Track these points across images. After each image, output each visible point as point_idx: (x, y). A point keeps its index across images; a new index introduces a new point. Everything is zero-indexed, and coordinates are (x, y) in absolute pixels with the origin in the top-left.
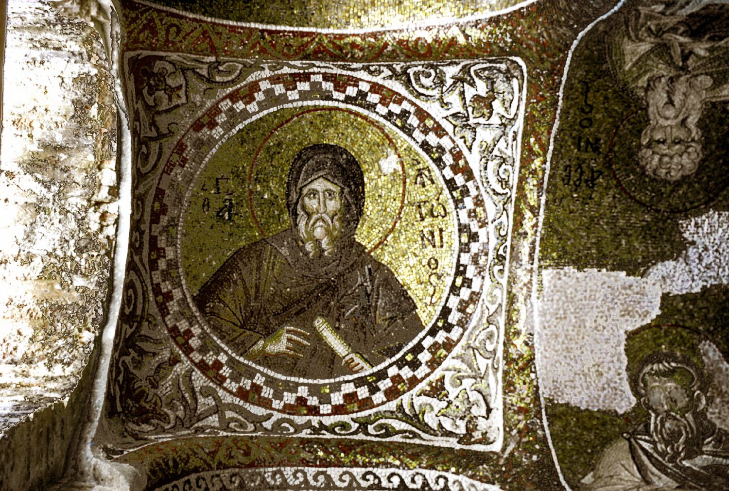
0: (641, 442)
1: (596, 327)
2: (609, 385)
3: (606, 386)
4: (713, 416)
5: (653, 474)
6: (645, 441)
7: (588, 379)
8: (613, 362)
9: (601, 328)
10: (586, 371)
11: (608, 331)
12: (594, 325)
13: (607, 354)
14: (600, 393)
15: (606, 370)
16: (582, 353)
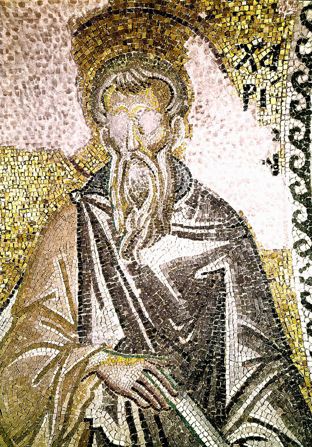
0: (95, 210)
1: (26, 15)
2: (55, 108)
3: (51, 111)
4: (192, 157)
5: (97, 290)
6: (98, 205)
7: (25, 102)
8: (58, 71)
9: (33, 16)
10: (21, 87)
11: (45, 20)
12: (21, 11)
13: (48, 59)
14: (42, 122)
15: (50, 85)
16: (11, 58)
